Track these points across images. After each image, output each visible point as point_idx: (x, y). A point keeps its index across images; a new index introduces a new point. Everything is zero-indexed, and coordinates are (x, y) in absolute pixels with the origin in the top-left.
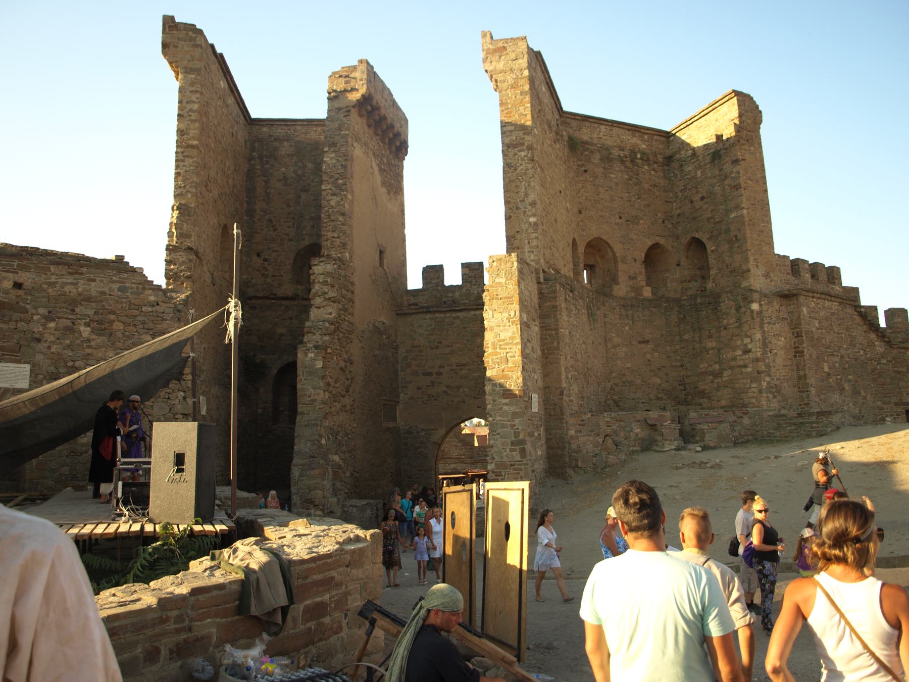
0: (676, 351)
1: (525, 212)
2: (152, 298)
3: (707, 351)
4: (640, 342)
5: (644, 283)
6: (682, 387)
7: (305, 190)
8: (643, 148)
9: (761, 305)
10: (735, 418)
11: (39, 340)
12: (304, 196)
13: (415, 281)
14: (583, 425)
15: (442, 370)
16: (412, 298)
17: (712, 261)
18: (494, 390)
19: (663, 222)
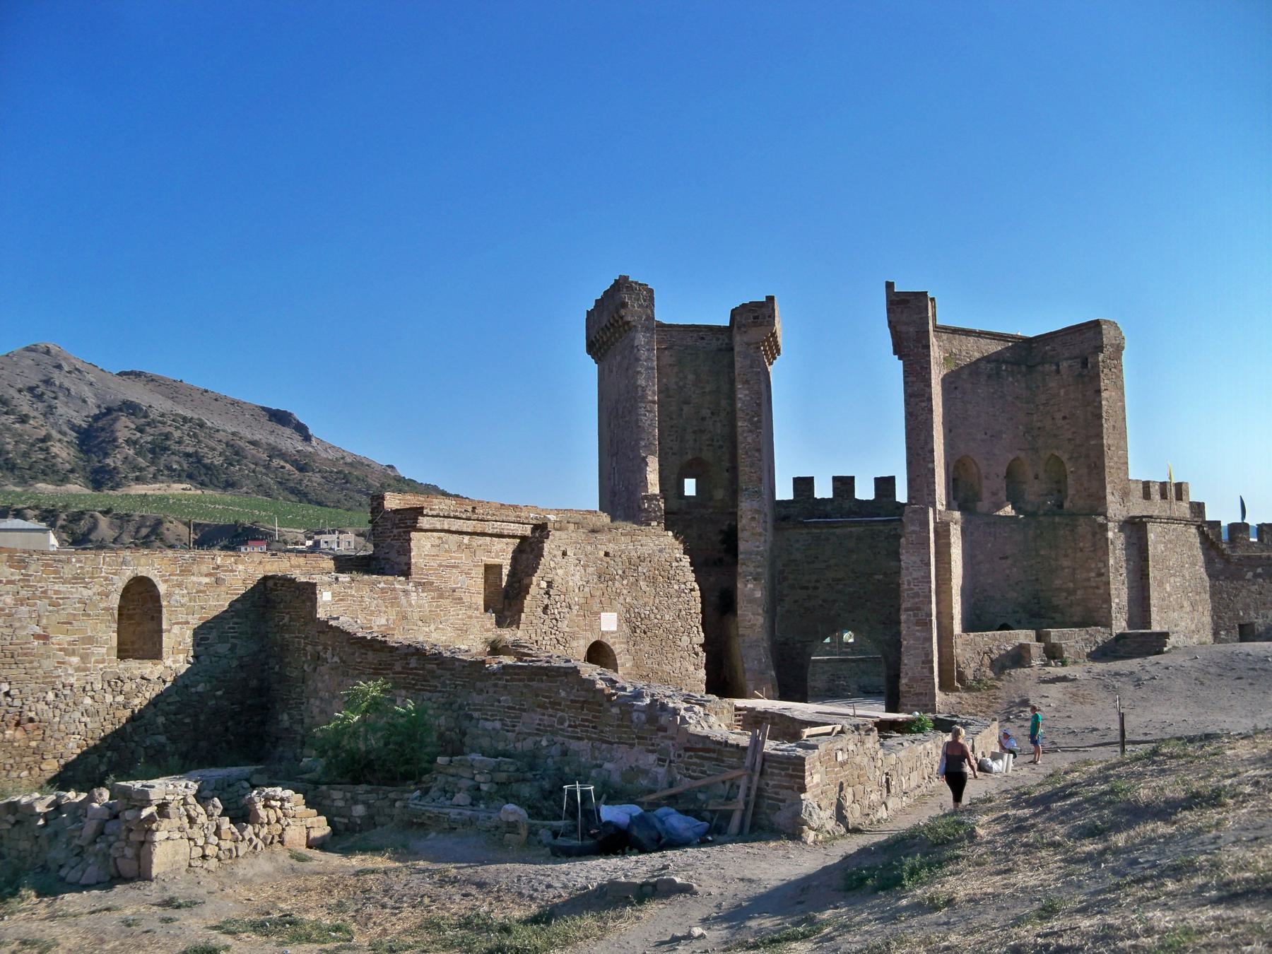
0: (1032, 565)
1: (924, 458)
2: (678, 555)
3: (1063, 569)
4: (1001, 558)
5: (1005, 498)
6: (1036, 601)
7: (687, 402)
8: (1008, 357)
9: (1114, 533)
10: (1088, 636)
11: (619, 594)
12: (686, 408)
13: (784, 492)
14: (967, 644)
15: (818, 584)
16: (783, 510)
17: (1070, 481)
18: (908, 619)
19: (1024, 435)
